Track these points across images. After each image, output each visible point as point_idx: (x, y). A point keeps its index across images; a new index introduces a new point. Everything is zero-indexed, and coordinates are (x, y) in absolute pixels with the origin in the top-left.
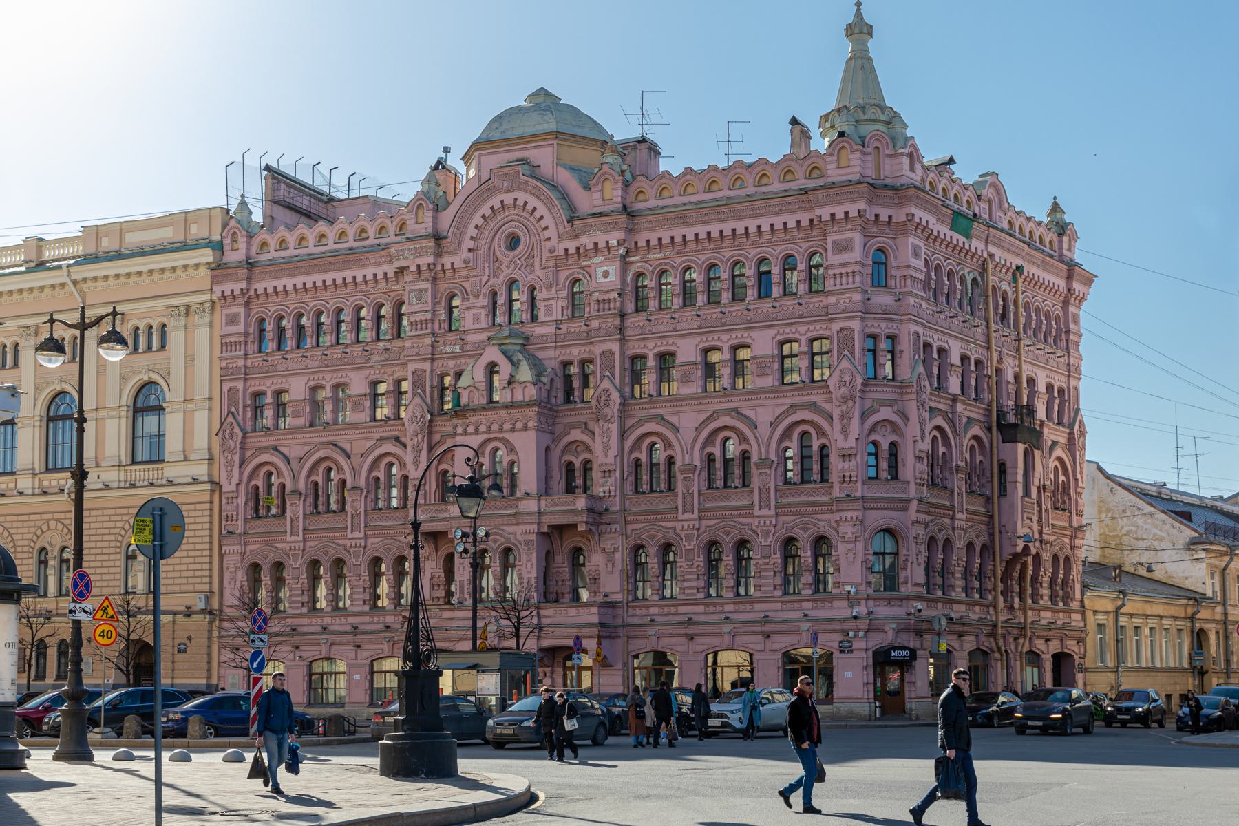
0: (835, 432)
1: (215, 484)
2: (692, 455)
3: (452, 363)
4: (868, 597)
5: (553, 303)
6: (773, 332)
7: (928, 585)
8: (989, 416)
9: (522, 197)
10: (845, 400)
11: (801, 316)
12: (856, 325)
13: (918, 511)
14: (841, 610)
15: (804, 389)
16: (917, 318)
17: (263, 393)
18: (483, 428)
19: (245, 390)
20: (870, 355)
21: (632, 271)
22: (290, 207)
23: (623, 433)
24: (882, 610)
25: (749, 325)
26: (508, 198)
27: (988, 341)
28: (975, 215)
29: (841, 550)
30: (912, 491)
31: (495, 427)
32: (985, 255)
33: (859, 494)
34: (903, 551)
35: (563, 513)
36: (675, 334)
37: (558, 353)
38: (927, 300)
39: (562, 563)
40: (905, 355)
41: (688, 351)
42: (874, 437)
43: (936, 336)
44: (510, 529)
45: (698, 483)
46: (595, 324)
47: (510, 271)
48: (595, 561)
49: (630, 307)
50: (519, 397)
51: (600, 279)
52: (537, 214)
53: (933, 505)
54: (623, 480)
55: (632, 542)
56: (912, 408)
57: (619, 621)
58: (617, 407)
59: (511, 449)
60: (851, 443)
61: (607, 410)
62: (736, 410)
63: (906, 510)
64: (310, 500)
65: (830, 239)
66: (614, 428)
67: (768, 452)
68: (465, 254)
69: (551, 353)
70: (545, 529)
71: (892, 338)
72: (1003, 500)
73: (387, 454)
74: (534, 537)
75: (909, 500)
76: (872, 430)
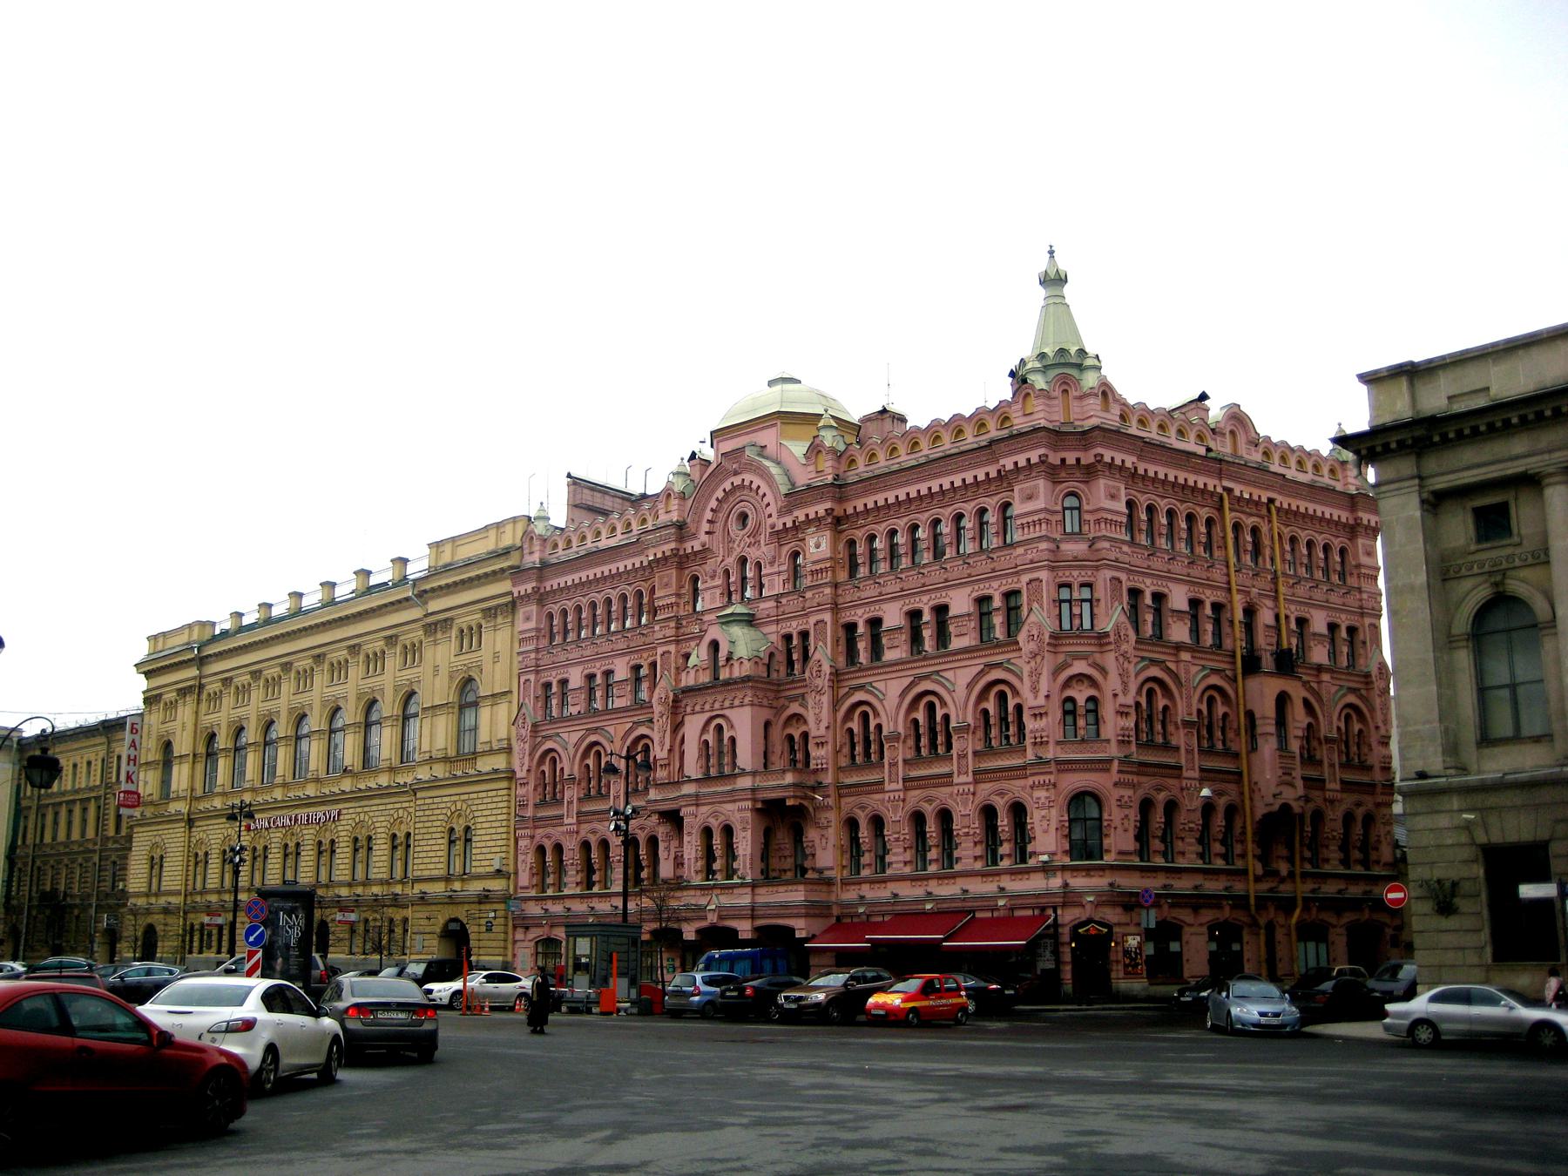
0: (1025, 689)
1: (510, 775)
2: (896, 722)
3: (693, 644)
4: (1064, 868)
6: (968, 590)
7: (1143, 850)
8: (1234, 663)
9: (748, 477)
11: (993, 571)
12: (1044, 575)
13: (1120, 772)
15: (998, 646)
16: (1116, 565)
18: (707, 707)
19: (537, 681)
20: (1065, 606)
21: (844, 537)
22: (592, 509)
23: (836, 704)
24: (1078, 882)
25: (948, 585)
27: (1229, 583)
28: (1209, 450)
29: (1035, 819)
30: (1113, 751)
31: (717, 705)
32: (1219, 490)
33: (1050, 756)
34: (1105, 816)
35: (774, 788)
38: (1132, 542)
39: (783, 838)
40: (1102, 603)
41: (893, 616)
42: (1069, 693)
43: (1148, 581)
44: (729, 806)
45: (902, 752)
46: (809, 595)
48: (811, 834)
49: (843, 576)
50: (736, 674)
51: (813, 550)
52: (761, 492)
53: (1142, 764)
54: (837, 752)
55: (844, 815)
56: (1110, 660)
57: (833, 899)
60: (1041, 701)
61: (819, 682)
62: (937, 672)
63: (1108, 770)
64: (584, 784)
65: (1016, 488)
66: (825, 699)
67: (965, 714)
68: (704, 538)
69: (773, 628)
70: (759, 805)
71: (1089, 585)
72: (1253, 756)
73: (643, 736)
74: (749, 814)
75: (1110, 761)
76: (1067, 684)
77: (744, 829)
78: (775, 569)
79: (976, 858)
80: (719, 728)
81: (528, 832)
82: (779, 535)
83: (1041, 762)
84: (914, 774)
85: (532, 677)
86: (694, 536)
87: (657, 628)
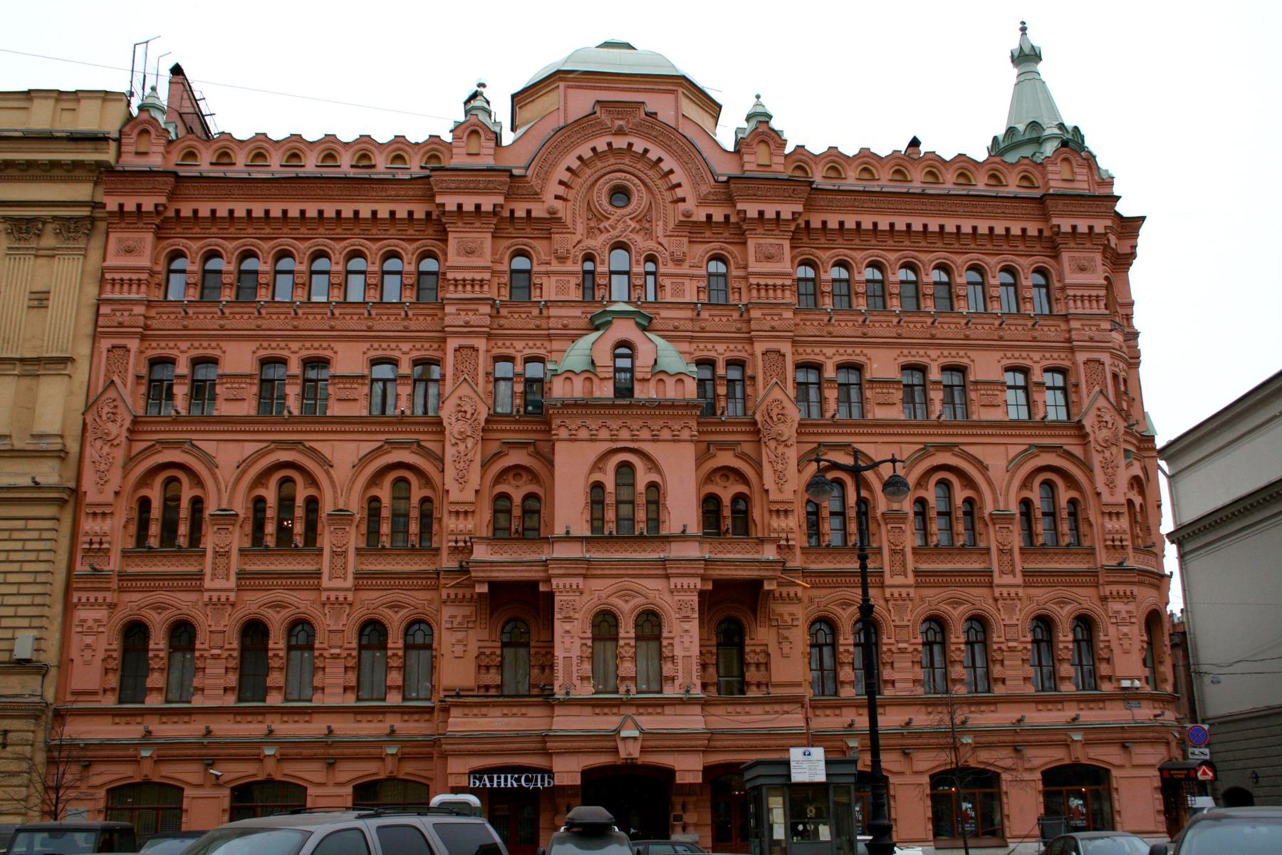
1: (72, 497)
5: (687, 282)
10: (1108, 444)
14: (1114, 714)
17: (171, 361)
26: (620, 143)
29: (1108, 634)
36: (866, 342)
37: (694, 346)
41: (882, 364)
47: (615, 233)
58: (796, 425)
59: (652, 464)
61: (781, 428)
66: (792, 454)
70: (709, 586)
77: (686, 619)
78: (685, 269)
79: (1026, 679)
80: (625, 467)
81: (110, 597)
82: (691, 229)
83: (1120, 568)
84: (924, 567)
85: (133, 344)
86: (536, 196)
87: (449, 309)
